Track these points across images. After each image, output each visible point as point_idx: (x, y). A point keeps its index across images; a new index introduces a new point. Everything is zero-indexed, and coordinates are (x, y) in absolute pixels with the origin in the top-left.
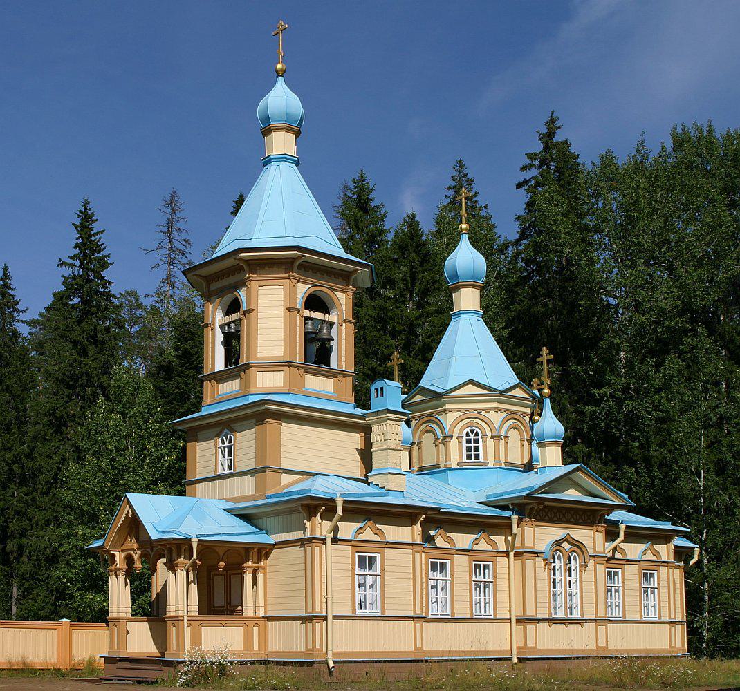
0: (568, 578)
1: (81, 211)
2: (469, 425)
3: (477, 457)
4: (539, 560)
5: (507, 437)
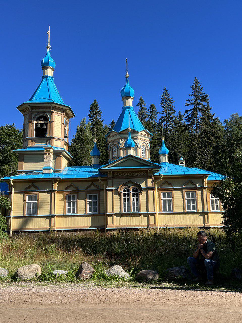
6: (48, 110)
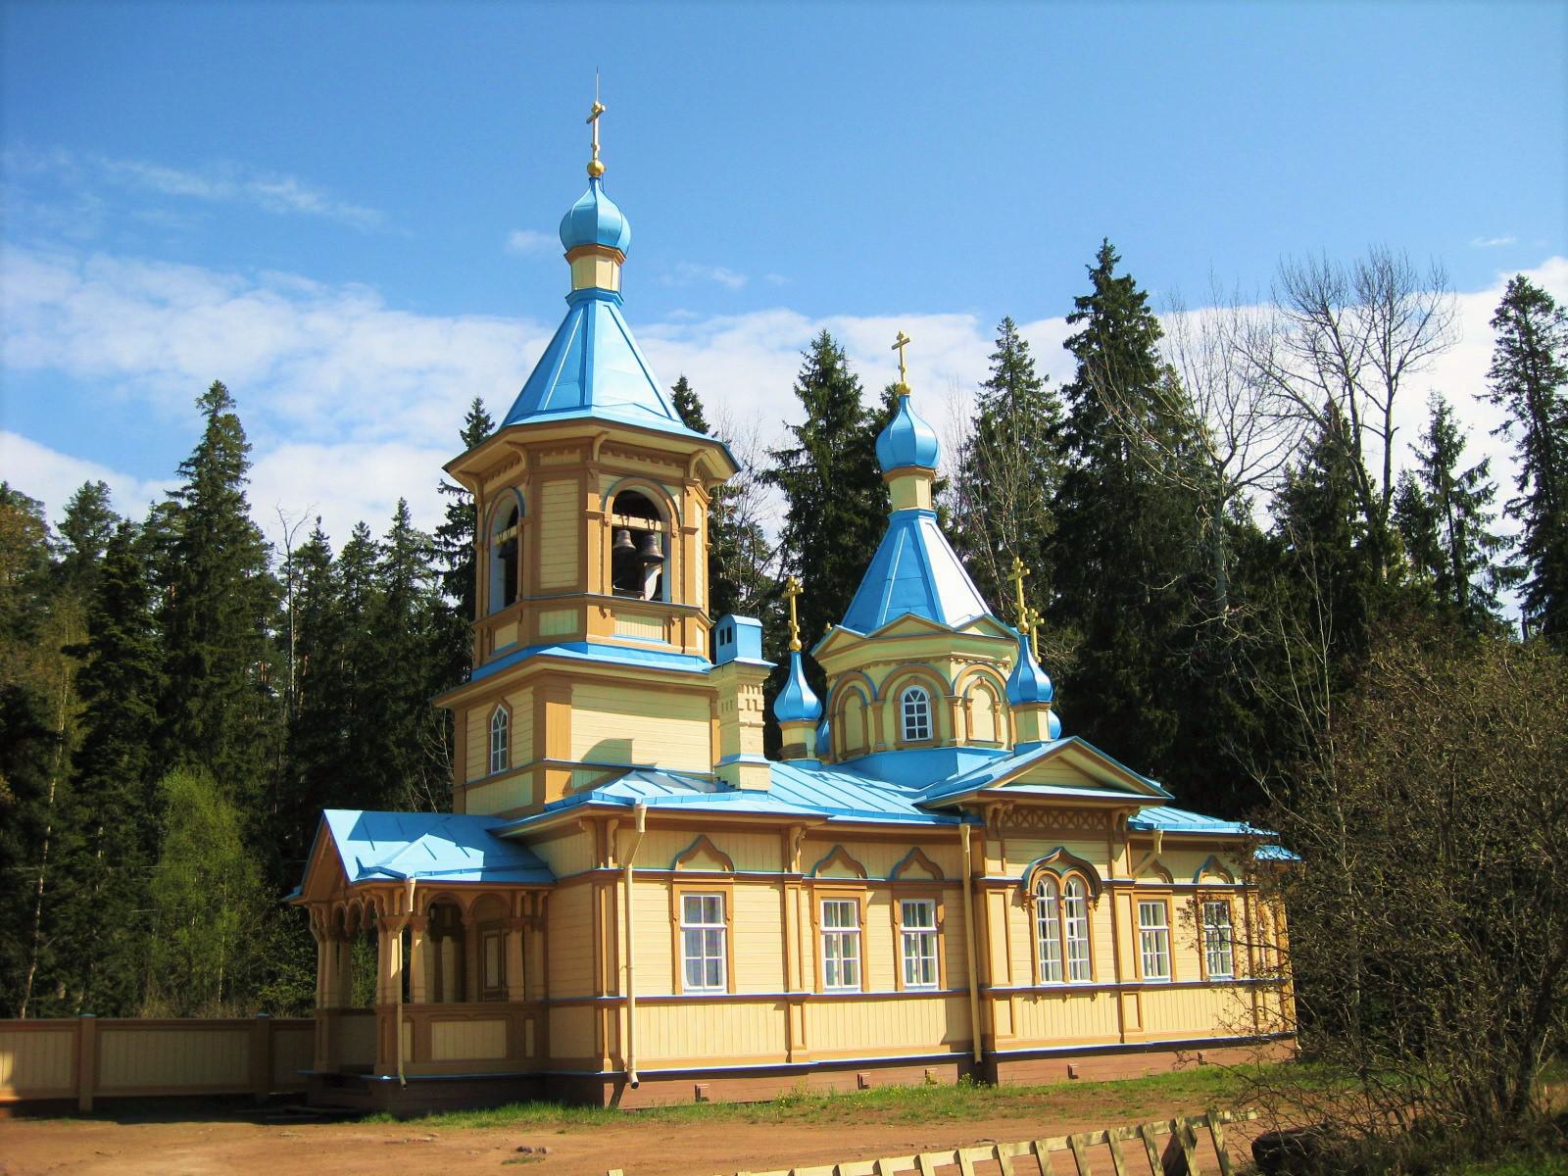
0: (1067, 921)
1: (470, 415)
3: (923, 733)
4: (1010, 892)
5: (967, 702)
6: (675, 472)
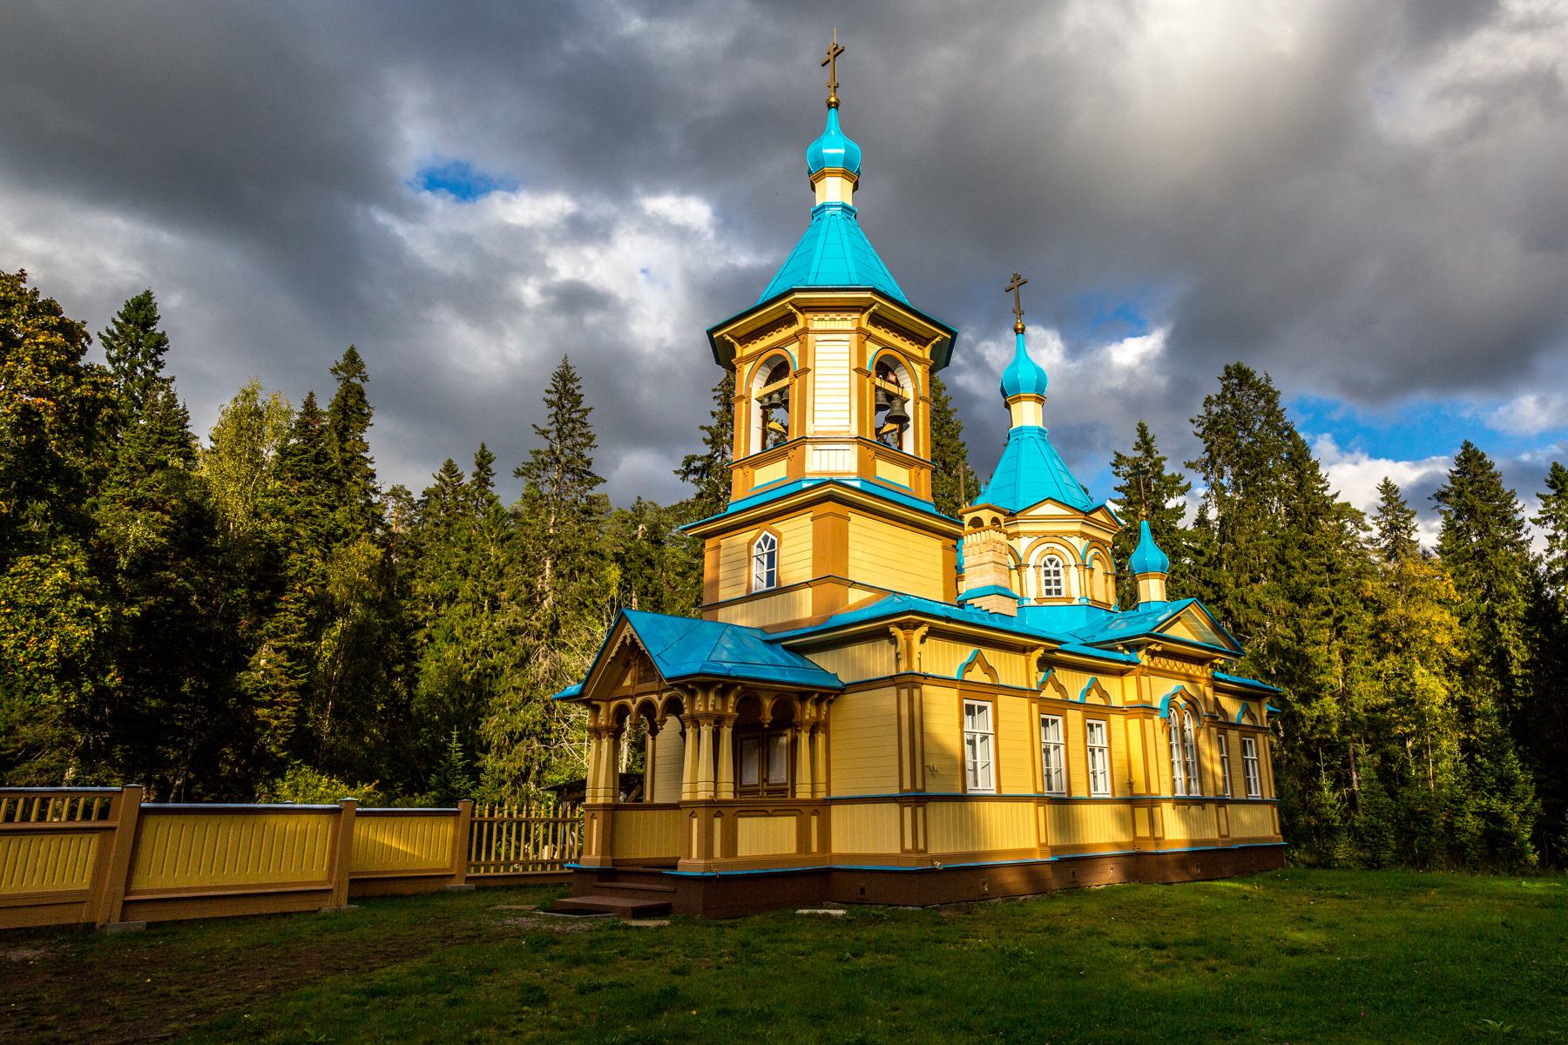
2: (1048, 552)
3: (1058, 592)
